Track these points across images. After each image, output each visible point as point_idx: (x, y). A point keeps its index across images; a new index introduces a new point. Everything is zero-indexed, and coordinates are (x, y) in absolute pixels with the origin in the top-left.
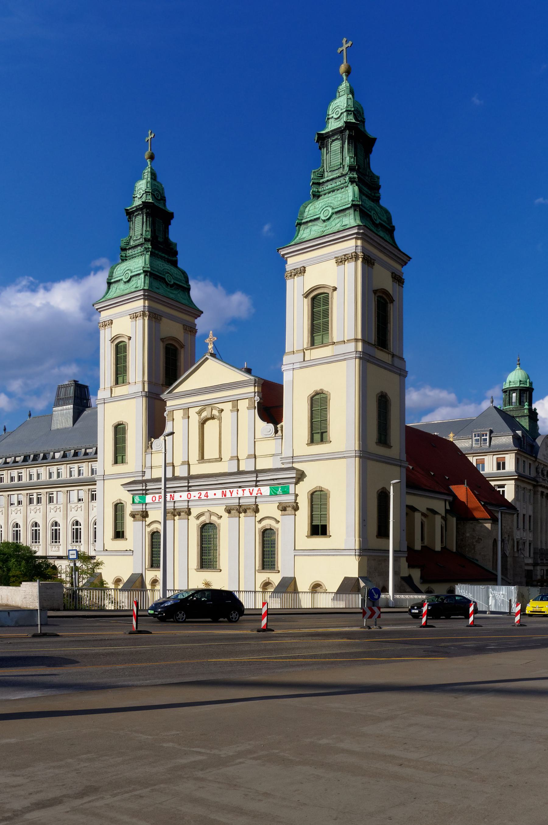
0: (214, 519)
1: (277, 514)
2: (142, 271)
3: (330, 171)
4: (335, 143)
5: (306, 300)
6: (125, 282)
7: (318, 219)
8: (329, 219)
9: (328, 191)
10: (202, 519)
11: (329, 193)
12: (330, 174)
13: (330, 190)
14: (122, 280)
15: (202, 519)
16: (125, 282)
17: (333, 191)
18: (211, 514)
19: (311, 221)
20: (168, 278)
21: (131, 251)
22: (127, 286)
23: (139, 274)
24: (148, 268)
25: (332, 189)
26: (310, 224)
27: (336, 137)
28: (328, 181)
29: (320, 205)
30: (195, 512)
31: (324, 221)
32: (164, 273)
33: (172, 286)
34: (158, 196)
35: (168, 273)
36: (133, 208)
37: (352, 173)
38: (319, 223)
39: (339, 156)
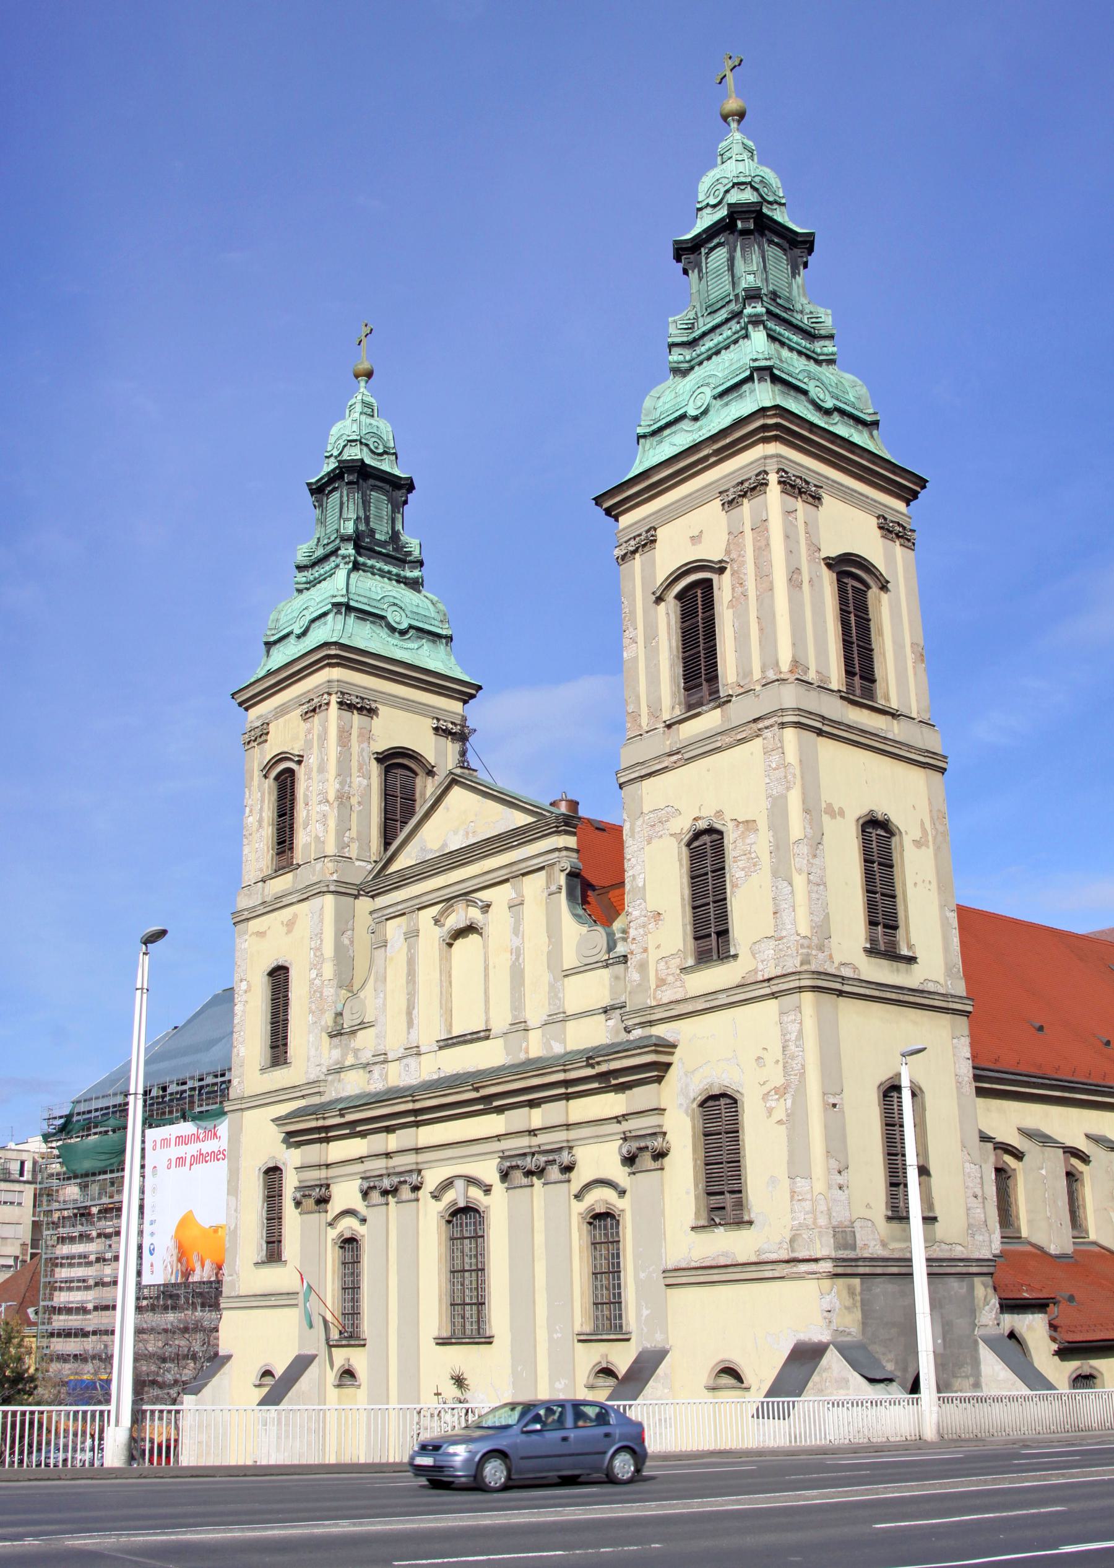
0: (475, 1193)
2: (330, 606)
3: (709, 314)
4: (714, 255)
6: (299, 637)
7: (683, 417)
8: (705, 412)
10: (450, 1196)
11: (709, 358)
12: (708, 319)
13: (710, 352)
14: (291, 633)
17: (717, 353)
18: (471, 1181)
20: (393, 617)
23: (325, 614)
24: (342, 596)
25: (714, 350)
27: (716, 241)
28: (704, 335)
29: (688, 388)
30: (432, 1178)
32: (385, 607)
33: (403, 633)
34: (377, 448)
35: (395, 604)
36: (322, 478)
37: (753, 305)
38: (685, 425)
39: (727, 278)
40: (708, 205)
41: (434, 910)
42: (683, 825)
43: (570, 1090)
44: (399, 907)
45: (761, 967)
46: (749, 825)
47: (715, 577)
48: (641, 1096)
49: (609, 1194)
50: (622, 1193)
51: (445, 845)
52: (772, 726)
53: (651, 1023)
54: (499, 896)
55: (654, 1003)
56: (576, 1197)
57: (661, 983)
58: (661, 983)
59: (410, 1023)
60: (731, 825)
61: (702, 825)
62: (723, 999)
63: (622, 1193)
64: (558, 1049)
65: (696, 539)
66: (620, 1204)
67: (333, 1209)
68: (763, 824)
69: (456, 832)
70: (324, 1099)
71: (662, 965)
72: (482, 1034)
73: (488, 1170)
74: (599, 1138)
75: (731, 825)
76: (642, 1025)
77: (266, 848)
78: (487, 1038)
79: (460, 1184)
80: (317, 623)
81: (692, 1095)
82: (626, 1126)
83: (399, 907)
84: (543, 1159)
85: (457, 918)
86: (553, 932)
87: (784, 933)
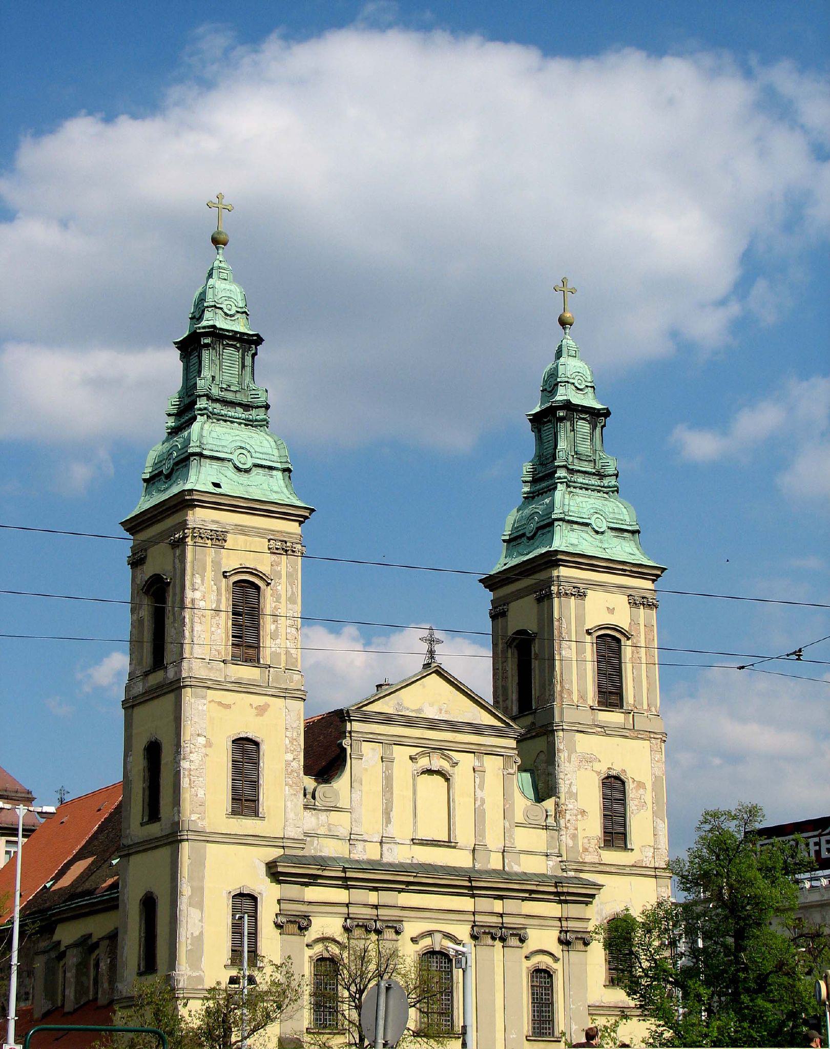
1: (556, 949)
4: (580, 423)
5: (588, 638)
7: (587, 525)
9: (580, 485)
11: (581, 488)
12: (576, 461)
14: (230, 460)
15: (426, 942)
16: (239, 469)
19: (577, 523)
21: (218, 405)
22: (243, 478)
26: (575, 526)
28: (579, 471)
30: (411, 928)
31: (597, 532)
40: (573, 384)
41: (414, 751)
42: (603, 768)
43: (532, 895)
44: (379, 737)
45: (645, 859)
46: (641, 785)
47: (623, 639)
48: (573, 910)
49: (548, 960)
50: (556, 960)
51: (420, 710)
52: (657, 739)
53: (581, 871)
54: (466, 761)
55: (581, 861)
56: (526, 957)
57: (586, 850)
58: (586, 850)
59: (388, 819)
60: (631, 780)
61: (613, 773)
62: (628, 870)
63: (556, 960)
64: (516, 869)
65: (611, 611)
66: (557, 966)
67: (309, 935)
68: (649, 786)
69: (432, 705)
70: (305, 853)
71: (586, 841)
72: (453, 844)
73: (462, 931)
74: (541, 927)
75: (631, 780)
76: (576, 870)
77: (224, 635)
78: (454, 847)
79: (438, 936)
80: (260, 470)
81: (604, 916)
82: (564, 924)
83: (379, 737)
84: (573, 936)
85: (438, 762)
86: (507, 796)
87: (659, 847)
